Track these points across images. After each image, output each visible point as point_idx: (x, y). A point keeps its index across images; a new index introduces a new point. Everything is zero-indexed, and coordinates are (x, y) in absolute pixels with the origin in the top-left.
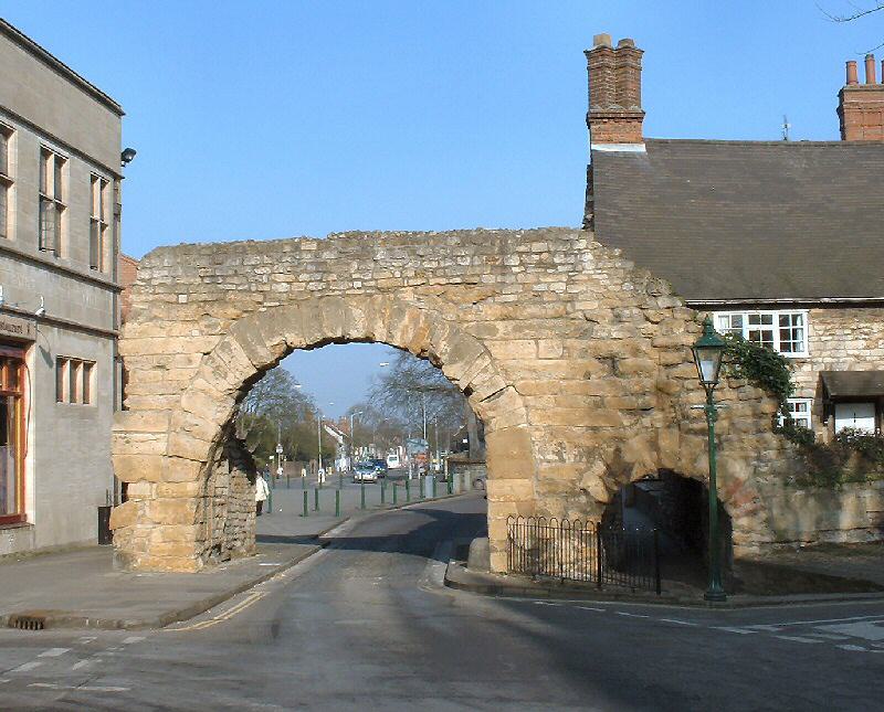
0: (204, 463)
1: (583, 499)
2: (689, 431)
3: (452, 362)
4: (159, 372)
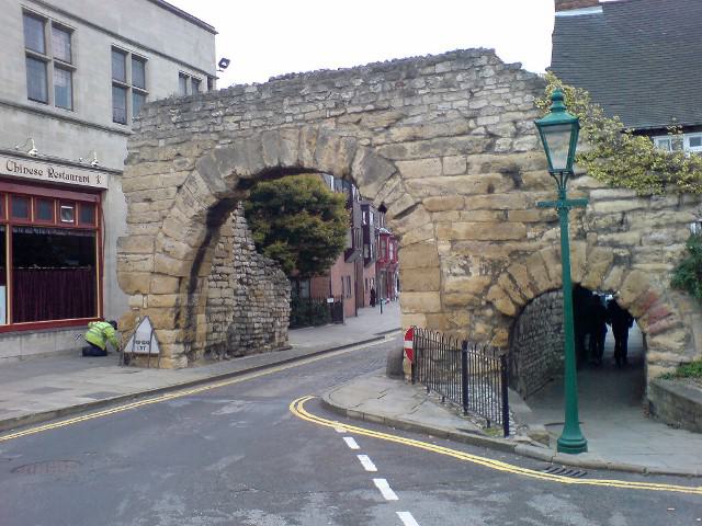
0: (181, 278)
1: (489, 312)
2: (596, 244)
3: (367, 183)
4: (145, 204)
